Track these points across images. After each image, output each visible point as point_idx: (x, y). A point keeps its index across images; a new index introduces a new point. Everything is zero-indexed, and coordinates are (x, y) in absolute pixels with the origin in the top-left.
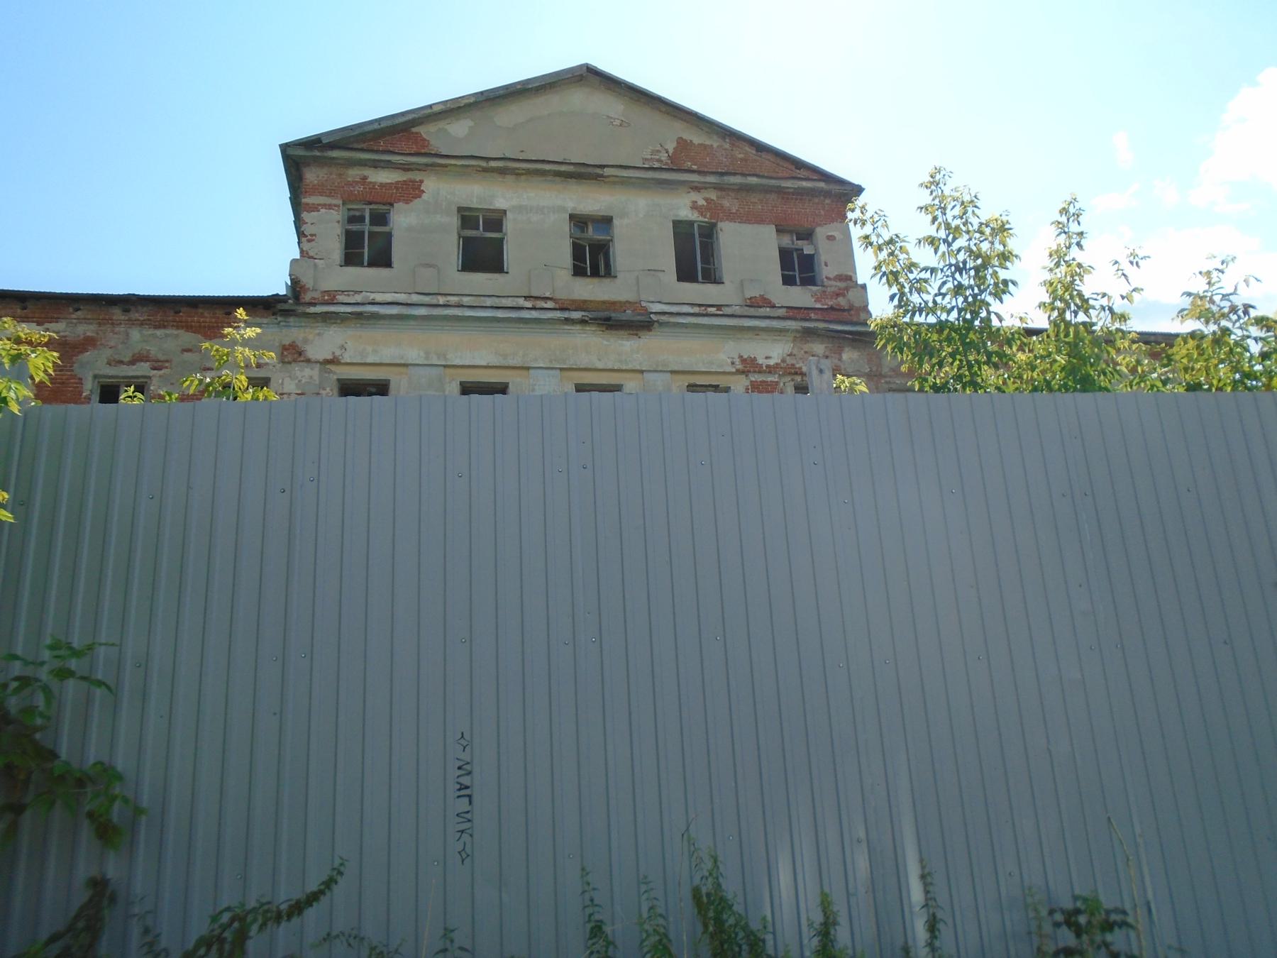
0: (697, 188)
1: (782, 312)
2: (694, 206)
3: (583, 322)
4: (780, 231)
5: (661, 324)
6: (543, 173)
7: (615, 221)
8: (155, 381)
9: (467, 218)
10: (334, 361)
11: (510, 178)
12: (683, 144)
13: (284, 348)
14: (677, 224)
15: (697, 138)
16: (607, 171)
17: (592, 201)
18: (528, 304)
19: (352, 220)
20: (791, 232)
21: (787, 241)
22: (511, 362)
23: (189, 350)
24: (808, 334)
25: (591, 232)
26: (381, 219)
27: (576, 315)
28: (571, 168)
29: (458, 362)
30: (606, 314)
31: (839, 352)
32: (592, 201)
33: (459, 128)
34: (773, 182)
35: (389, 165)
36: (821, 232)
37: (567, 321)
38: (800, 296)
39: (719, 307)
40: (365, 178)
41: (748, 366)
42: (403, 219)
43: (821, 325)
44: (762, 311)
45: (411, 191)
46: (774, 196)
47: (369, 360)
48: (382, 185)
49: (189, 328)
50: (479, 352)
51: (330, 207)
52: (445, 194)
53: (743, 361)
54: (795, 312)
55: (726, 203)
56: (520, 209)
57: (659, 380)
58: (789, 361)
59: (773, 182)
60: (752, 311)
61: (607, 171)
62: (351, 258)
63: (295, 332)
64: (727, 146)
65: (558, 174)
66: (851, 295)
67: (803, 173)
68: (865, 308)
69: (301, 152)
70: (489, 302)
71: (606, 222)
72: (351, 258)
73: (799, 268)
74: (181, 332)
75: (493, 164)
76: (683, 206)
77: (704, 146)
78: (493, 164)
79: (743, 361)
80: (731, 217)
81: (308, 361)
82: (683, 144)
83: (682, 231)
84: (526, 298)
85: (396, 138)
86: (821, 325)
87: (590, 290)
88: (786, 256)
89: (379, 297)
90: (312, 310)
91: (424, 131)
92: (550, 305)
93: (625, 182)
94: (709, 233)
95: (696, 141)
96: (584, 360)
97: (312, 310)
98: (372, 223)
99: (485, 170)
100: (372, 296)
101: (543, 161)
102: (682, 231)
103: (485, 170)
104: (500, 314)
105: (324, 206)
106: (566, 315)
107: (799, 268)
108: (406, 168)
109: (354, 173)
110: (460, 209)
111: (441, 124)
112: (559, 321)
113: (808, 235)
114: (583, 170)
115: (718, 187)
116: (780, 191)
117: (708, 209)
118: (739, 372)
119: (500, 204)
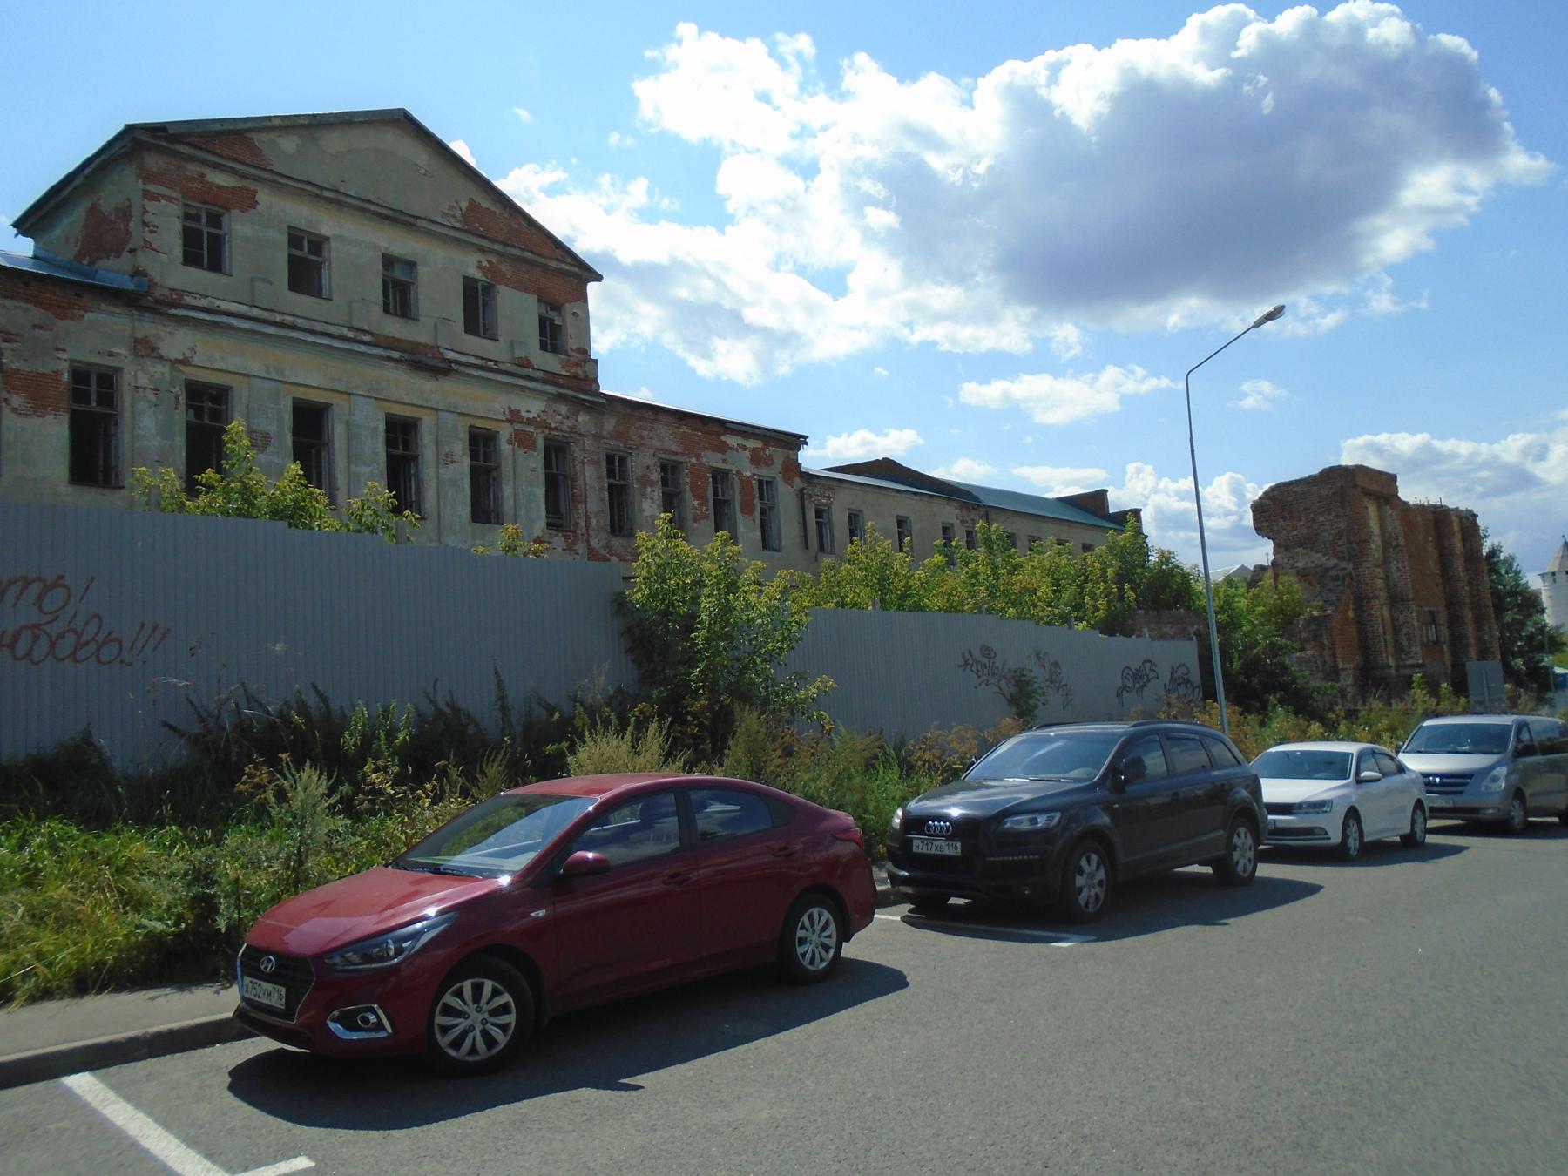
0: (483, 250)
1: (539, 374)
2: (480, 267)
3: (399, 361)
5: (457, 371)
7: (419, 267)
8: (6, 354)
9: (295, 238)
10: (185, 362)
12: (473, 205)
13: (137, 341)
14: (465, 278)
15: (485, 203)
16: (420, 223)
17: (403, 244)
18: (351, 335)
19: (187, 216)
22: (338, 387)
23: (40, 327)
24: (560, 397)
26: (215, 220)
27: (396, 355)
28: (390, 213)
29: (292, 379)
30: (417, 357)
31: (576, 413)
32: (403, 244)
33: (289, 144)
34: (543, 260)
35: (232, 171)
37: (389, 359)
38: (550, 362)
39: (496, 362)
40: (203, 176)
41: (515, 417)
42: (239, 227)
43: (570, 393)
44: (528, 372)
45: (247, 201)
47: (218, 366)
48: (220, 188)
49: (37, 302)
50: (311, 375)
51: (170, 199)
53: (511, 412)
54: (550, 378)
55: (503, 268)
57: (449, 419)
58: (543, 417)
60: (519, 370)
61: (420, 223)
62: (191, 259)
63: (148, 327)
66: (588, 366)
67: (559, 253)
68: (595, 380)
69: (146, 138)
70: (319, 327)
71: (411, 265)
72: (191, 259)
73: (551, 336)
74: (30, 306)
75: (327, 194)
76: (471, 264)
78: (327, 194)
79: (511, 412)
81: (161, 358)
83: (470, 286)
84: (351, 328)
86: (570, 393)
87: (394, 328)
89: (224, 305)
90: (173, 311)
91: (260, 139)
92: (367, 338)
94: (488, 289)
96: (396, 393)
97: (173, 311)
98: (208, 224)
99: (317, 196)
100: (218, 303)
101: (369, 201)
102: (470, 286)
103: (317, 196)
104: (336, 344)
105: (164, 197)
106: (388, 353)
107: (551, 336)
108: (243, 176)
109: (193, 169)
111: (272, 135)
112: (376, 356)
116: (545, 267)
118: (508, 421)
119: (325, 230)
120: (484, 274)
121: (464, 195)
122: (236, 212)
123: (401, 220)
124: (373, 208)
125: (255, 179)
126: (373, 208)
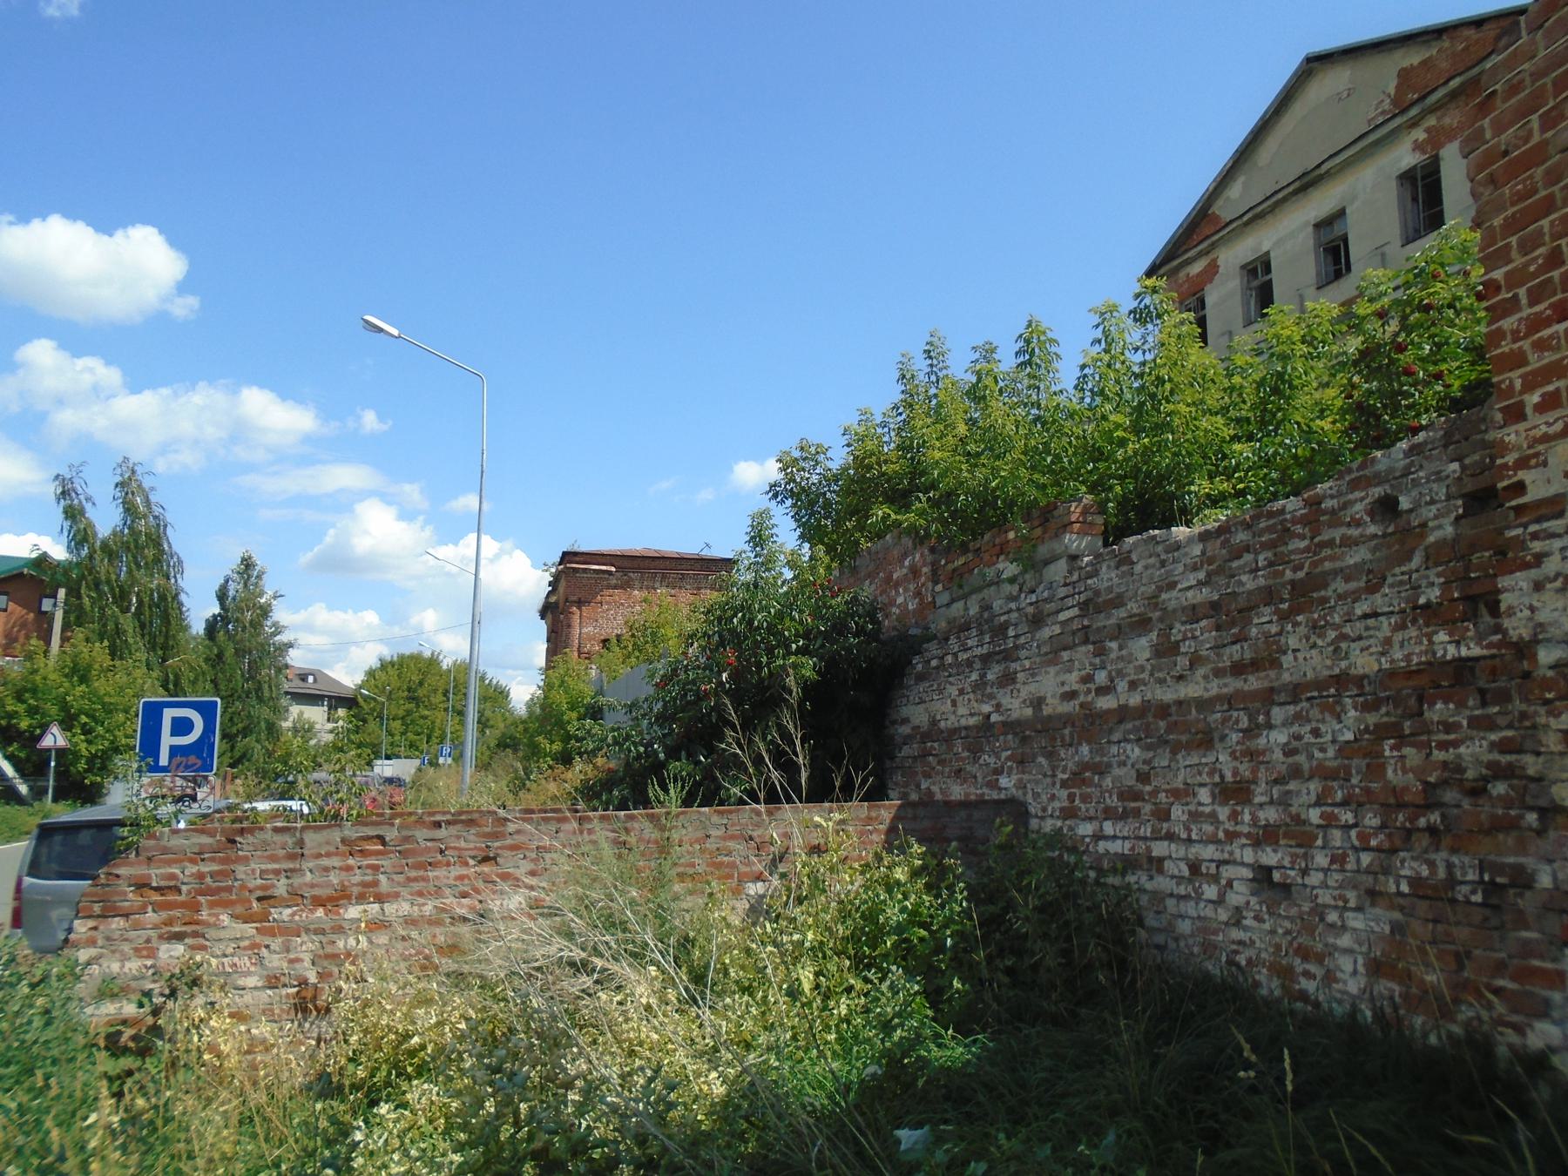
0: (1413, 124)
2: (1418, 146)
6: (1285, 200)
11: (1269, 218)
25: (1337, 230)
28: (1297, 184)
33: (1235, 191)
45: (1212, 269)
48: (1198, 275)
52: (1234, 255)
55: (1447, 121)
56: (1279, 242)
65: (1296, 193)
75: (1245, 218)
76: (1404, 156)
77: (1424, 63)
78: (1245, 218)
82: (1405, 75)
85: (1200, 230)
108: (1206, 252)
109: (1182, 275)
110: (1243, 267)
114: (1306, 180)
115: (1432, 110)
120: (1424, 152)
122: (1208, 288)
123: (1308, 182)
124: (1280, 196)
125: (1213, 246)
126: (1280, 196)
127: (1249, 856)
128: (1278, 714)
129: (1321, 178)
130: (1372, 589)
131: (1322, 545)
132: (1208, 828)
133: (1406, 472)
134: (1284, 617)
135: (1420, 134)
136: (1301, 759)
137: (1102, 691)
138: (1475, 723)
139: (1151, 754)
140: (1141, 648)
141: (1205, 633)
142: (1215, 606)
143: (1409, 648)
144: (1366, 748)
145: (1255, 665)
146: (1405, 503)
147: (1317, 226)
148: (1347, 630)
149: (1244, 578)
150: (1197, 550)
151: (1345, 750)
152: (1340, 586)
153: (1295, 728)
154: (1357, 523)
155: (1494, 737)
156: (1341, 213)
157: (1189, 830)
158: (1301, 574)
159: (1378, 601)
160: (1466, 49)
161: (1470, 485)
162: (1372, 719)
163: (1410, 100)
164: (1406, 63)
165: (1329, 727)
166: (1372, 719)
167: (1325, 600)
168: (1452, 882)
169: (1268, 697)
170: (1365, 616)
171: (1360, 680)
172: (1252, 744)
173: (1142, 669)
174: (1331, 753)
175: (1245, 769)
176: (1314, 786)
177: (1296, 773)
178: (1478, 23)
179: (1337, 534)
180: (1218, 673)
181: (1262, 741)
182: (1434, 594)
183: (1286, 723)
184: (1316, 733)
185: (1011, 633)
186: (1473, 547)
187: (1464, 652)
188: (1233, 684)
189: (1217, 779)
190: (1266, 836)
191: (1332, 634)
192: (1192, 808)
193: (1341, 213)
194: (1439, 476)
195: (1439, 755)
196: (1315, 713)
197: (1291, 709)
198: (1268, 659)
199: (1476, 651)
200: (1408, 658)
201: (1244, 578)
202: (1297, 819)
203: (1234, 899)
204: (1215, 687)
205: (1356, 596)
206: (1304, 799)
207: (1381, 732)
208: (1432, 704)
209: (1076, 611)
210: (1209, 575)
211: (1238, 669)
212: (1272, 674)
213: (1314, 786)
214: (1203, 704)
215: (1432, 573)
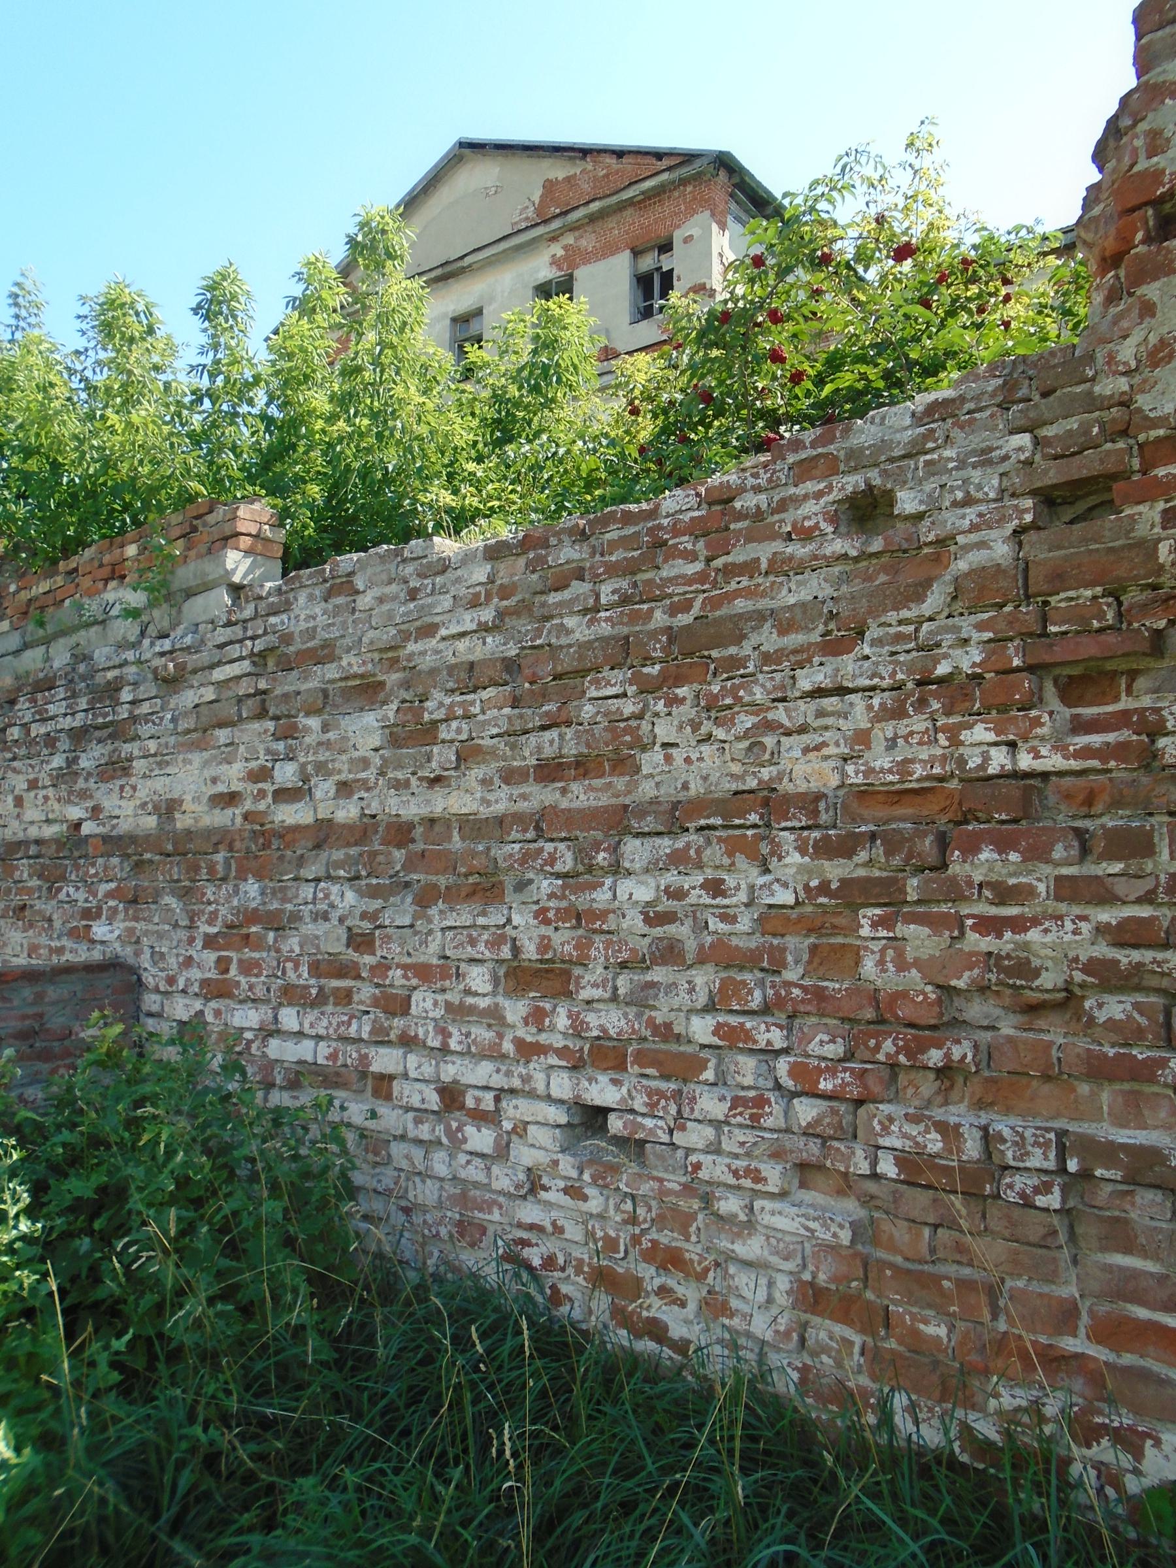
0: (554, 239)
2: (555, 262)
4: (636, 253)
20: (652, 248)
21: (648, 262)
28: (439, 272)
34: (614, 199)
36: (678, 236)
46: (629, 211)
55: (583, 243)
59: (614, 199)
64: (590, 167)
67: (665, 163)
77: (568, 179)
80: (588, 258)
82: (550, 186)
88: (644, 283)
93: (489, 263)
95: (561, 175)
113: (666, 247)
114: (448, 269)
115: (572, 229)
116: (630, 203)
117: (566, 258)
121: (530, 181)
127: (562, 1085)
128: (635, 851)
129: (462, 271)
130: (833, 647)
131: (730, 571)
132: (482, 1034)
133: (915, 451)
134: (647, 688)
135: (557, 250)
136: (681, 931)
137: (284, 795)
138: (1066, 890)
139: (377, 904)
140: (365, 729)
141: (490, 711)
142: (511, 666)
143: (907, 750)
144: (824, 919)
145: (583, 767)
146: (907, 502)
147: (454, 320)
148: (779, 714)
149: (570, 622)
150: (480, 573)
151: (772, 920)
152: (768, 639)
153: (671, 878)
154: (806, 534)
155: (1107, 916)
156: (479, 312)
157: (445, 1034)
158: (684, 619)
159: (848, 667)
160: (607, 176)
161: (1052, 474)
162: (835, 870)
163: (553, 215)
164: (552, 175)
165: (743, 877)
166: (835, 870)
167: (736, 663)
168: (992, 1166)
169: (619, 822)
170: (818, 693)
171: (811, 802)
172: (581, 901)
173: (365, 763)
174: (745, 923)
175: (563, 940)
176: (705, 979)
177: (670, 953)
178: (620, 153)
179: (764, 552)
180: (510, 777)
181: (602, 897)
182: (969, 659)
183: (654, 867)
184: (715, 887)
185: (126, 695)
186: (1059, 579)
187: (1025, 762)
188: (541, 796)
189: (506, 952)
190: (606, 1055)
191: (746, 721)
192: (454, 997)
193: (479, 312)
194: (985, 458)
195: (977, 942)
196: (715, 853)
197: (665, 845)
198: (618, 754)
199: (1053, 761)
200: (903, 768)
201: (570, 622)
202: (666, 1032)
203: (525, 1155)
204: (502, 801)
205: (801, 659)
206: (682, 998)
207: (853, 894)
208: (971, 849)
209: (246, 666)
210: (501, 614)
211: (550, 771)
212: (620, 782)
213: (705, 979)
214: (472, 826)
215: (966, 625)
